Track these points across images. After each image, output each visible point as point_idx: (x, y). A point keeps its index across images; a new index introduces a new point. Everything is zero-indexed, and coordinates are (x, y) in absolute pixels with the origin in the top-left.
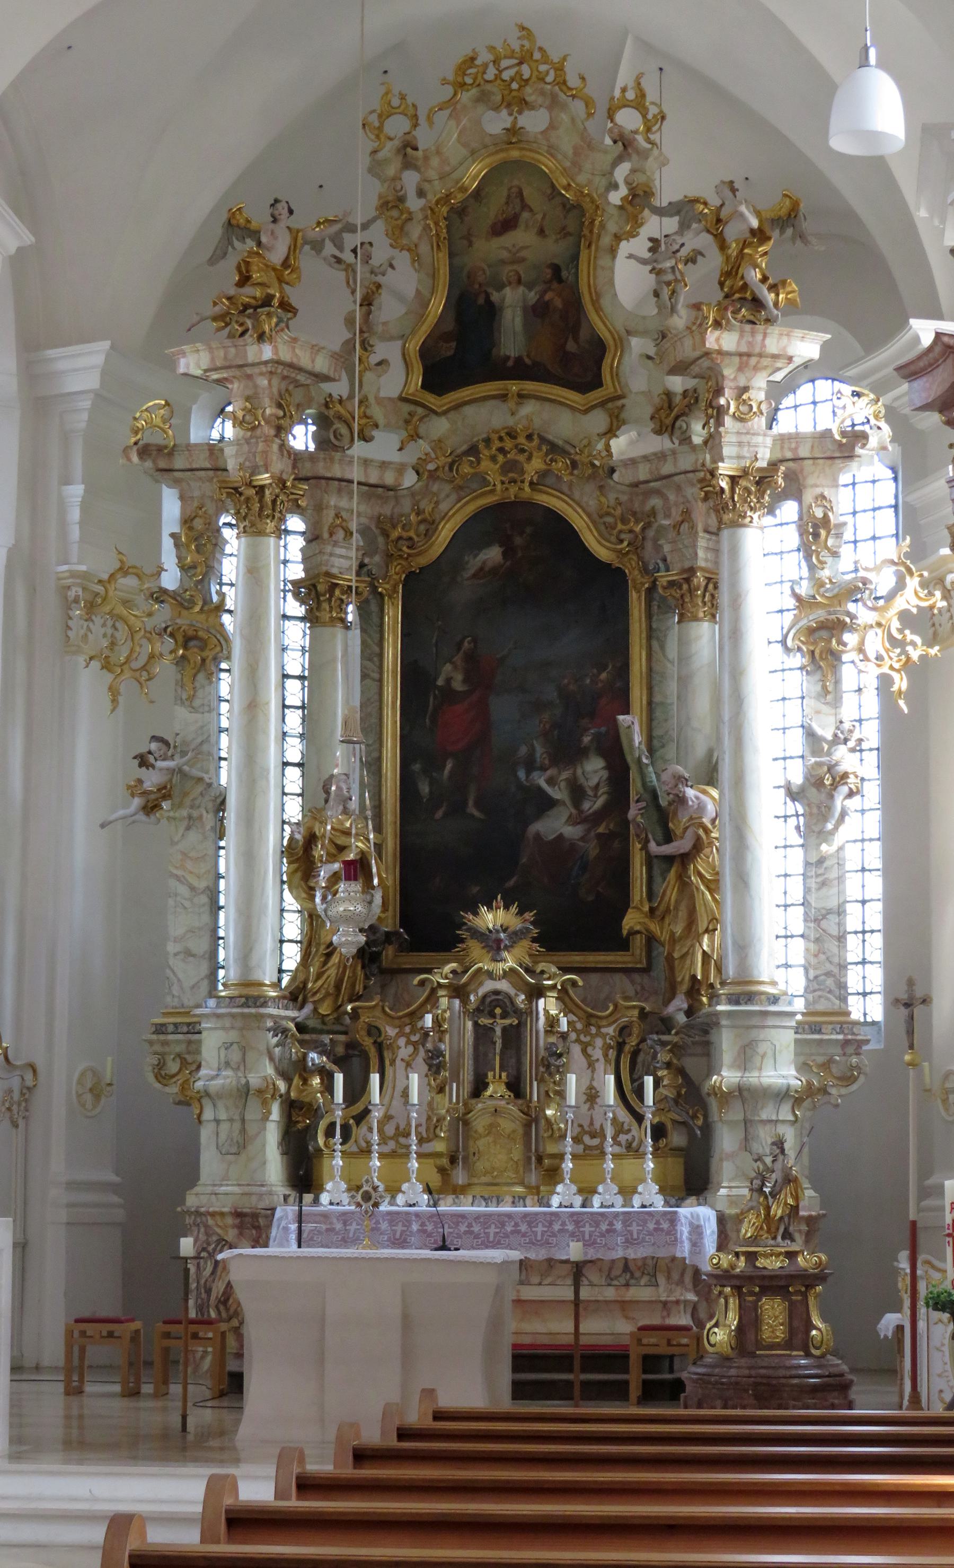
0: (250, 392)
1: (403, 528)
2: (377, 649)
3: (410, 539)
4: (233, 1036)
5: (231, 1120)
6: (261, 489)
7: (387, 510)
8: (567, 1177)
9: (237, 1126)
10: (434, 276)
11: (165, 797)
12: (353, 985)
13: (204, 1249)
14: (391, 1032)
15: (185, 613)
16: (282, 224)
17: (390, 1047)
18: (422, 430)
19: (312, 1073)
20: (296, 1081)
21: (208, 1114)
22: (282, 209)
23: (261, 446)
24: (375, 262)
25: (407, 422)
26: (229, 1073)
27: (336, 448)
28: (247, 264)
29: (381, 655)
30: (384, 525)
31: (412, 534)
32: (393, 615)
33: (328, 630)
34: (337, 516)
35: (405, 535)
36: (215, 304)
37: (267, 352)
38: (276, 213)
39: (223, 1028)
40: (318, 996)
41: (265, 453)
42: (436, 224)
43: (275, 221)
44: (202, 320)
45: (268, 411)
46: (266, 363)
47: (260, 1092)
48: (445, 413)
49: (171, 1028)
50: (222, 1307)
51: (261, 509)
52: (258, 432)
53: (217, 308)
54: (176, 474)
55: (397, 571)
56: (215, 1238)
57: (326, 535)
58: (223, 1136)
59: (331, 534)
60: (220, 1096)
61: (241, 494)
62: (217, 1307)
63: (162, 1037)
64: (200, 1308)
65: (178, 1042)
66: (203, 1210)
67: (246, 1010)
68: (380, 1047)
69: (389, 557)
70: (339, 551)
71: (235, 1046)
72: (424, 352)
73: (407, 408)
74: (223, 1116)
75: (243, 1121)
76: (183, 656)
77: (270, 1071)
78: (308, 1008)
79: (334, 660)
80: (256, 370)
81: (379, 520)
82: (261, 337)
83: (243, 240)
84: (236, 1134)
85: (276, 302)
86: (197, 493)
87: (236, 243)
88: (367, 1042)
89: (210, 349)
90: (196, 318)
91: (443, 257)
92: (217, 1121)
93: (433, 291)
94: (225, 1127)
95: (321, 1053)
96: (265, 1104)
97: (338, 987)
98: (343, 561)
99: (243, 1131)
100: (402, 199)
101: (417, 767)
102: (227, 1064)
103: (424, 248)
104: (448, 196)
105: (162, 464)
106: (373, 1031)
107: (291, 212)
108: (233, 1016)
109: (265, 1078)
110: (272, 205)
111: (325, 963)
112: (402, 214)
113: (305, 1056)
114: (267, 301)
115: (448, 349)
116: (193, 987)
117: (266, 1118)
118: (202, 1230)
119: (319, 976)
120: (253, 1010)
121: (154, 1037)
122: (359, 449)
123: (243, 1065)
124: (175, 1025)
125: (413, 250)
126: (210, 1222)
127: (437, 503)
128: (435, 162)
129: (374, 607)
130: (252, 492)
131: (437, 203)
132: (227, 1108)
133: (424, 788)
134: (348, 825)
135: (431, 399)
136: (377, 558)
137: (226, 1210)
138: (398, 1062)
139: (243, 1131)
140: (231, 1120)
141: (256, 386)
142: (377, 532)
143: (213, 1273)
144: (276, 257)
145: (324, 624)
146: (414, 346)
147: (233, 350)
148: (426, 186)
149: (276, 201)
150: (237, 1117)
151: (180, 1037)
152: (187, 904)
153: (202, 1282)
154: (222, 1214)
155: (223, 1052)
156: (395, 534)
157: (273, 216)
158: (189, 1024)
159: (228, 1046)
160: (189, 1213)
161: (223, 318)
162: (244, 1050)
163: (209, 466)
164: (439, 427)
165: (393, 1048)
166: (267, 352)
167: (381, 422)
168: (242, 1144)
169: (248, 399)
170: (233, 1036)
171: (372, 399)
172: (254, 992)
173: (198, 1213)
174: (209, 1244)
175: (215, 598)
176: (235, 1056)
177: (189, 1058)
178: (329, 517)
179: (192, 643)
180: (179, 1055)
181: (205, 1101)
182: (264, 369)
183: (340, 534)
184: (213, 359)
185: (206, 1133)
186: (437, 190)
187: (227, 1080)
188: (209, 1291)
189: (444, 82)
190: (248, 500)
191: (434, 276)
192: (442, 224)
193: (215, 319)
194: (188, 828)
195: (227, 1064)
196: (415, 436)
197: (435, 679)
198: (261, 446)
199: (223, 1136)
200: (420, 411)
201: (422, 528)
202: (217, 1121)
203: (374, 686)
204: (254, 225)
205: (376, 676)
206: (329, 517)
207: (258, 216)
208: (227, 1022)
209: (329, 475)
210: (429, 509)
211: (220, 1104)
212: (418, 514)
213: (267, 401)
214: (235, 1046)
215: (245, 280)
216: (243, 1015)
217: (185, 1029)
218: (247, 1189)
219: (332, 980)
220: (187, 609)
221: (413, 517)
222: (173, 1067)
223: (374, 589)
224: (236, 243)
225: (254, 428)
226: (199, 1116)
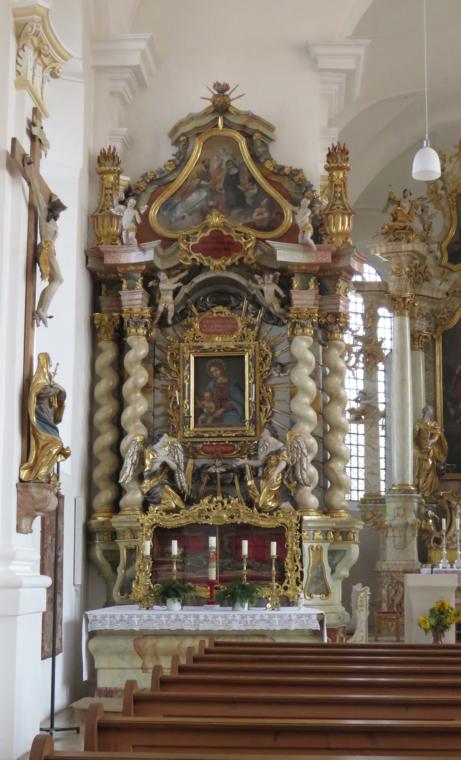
0: (399, 262)
1: (442, 314)
2: (433, 360)
3: (444, 318)
4: (400, 504)
5: (400, 536)
6: (404, 299)
7: (435, 307)
8: (444, 556)
9: (403, 538)
10: (451, 220)
11: (363, 415)
12: (435, 486)
13: (391, 585)
14: (455, 503)
15: (368, 345)
16: (407, 199)
17: (454, 508)
18: (448, 278)
19: (429, 518)
20: (424, 521)
21: (390, 534)
22: (407, 193)
23: (404, 282)
24: (429, 214)
25: (442, 274)
26: (399, 518)
27: (418, 283)
28: (396, 213)
29: (435, 362)
30: (434, 313)
31: (445, 316)
32: (439, 347)
33: (417, 352)
34: (420, 309)
35: (442, 317)
36: (383, 228)
37: (410, 247)
38: (405, 194)
39: (396, 502)
40: (424, 489)
41: (406, 285)
42: (452, 200)
43: (405, 197)
44: (378, 234)
45: (407, 269)
46: (408, 251)
47: (412, 525)
48: (457, 271)
49: (368, 501)
50: (399, 607)
51: (404, 306)
52: (402, 277)
53: (384, 230)
54: (364, 293)
55: (440, 330)
56: (395, 581)
57: (416, 317)
58: (397, 543)
59: (418, 316)
60: (396, 527)
61: (396, 300)
62: (397, 607)
63: (365, 505)
64: (389, 607)
65: (371, 506)
66: (391, 570)
67: (406, 495)
68: (450, 508)
69: (437, 326)
70: (421, 322)
71: (401, 508)
72: (449, 248)
73: (442, 269)
74: (397, 534)
75: (405, 536)
76: (368, 362)
77: (415, 518)
78: (421, 493)
79: (420, 364)
80: (403, 254)
81: (432, 311)
82: (408, 241)
83: (392, 205)
84: (402, 542)
85: (407, 228)
86: (370, 300)
87: (390, 206)
88: (446, 507)
89: (387, 246)
90: (375, 234)
91: (454, 213)
92: (394, 537)
93: (451, 226)
94: (397, 539)
95: (432, 511)
96: (414, 530)
97: (431, 487)
98: (423, 325)
99: (405, 540)
100: (437, 190)
101: (449, 404)
102: (398, 515)
103: (447, 209)
104: (456, 191)
105: (361, 289)
106: (449, 503)
107: (411, 194)
108: (401, 497)
109: (414, 520)
110: (404, 192)
111: (427, 477)
112: (438, 196)
113: (427, 512)
114: (404, 228)
115: (457, 248)
116: (375, 486)
117: (414, 535)
118: (390, 578)
119: (425, 481)
120: (409, 495)
121: (362, 505)
122: (426, 284)
123: (404, 515)
124: (370, 500)
125: (442, 210)
126: (393, 575)
127: (454, 305)
128: (450, 177)
129: (431, 344)
130: (401, 300)
131: (452, 192)
132: (399, 532)
133: (452, 412)
134: (433, 425)
135: (451, 266)
136: (432, 326)
137: (401, 570)
138: (457, 514)
139: (405, 540)
140: (400, 536)
141: (401, 260)
142: (431, 315)
143: (395, 594)
144: (406, 211)
145: (415, 350)
146: (444, 245)
147: (396, 246)
148: (447, 186)
149: (406, 190)
150: (403, 535)
151: (372, 505)
152: (372, 454)
153: (390, 597)
154: (399, 572)
155: (396, 511)
156: (438, 316)
157: (404, 195)
158: (375, 500)
159: (398, 508)
160: (384, 571)
161: (386, 234)
162: (405, 510)
163: (378, 289)
164: (454, 277)
165: (455, 509)
166: (410, 247)
167: (433, 275)
168: (405, 546)
169: (398, 264)
170: (400, 504)
171: (429, 265)
172: (406, 488)
173: (388, 571)
174: (392, 583)
175: (379, 340)
176: (401, 512)
177: (375, 513)
178: (416, 310)
179: (370, 356)
180: (371, 512)
181: (389, 529)
182: (406, 253)
183: (421, 316)
184: (387, 250)
185: (389, 541)
186: (451, 188)
187: (398, 521)
188: (393, 601)
189: (455, 147)
190: (398, 302)
191: (451, 220)
192: (454, 200)
193: (383, 234)
194: (371, 426)
195: (398, 515)
196: (446, 280)
197: (455, 371)
198: (404, 282)
199: (397, 543)
200: (447, 270)
201: (448, 314)
202: (394, 537)
203: (432, 373)
204: (398, 198)
205: (433, 369)
206: (416, 310)
207: (398, 196)
208: (398, 499)
209: (420, 294)
210: (451, 307)
211: (396, 531)
212: (447, 309)
213: (405, 265)
214: (401, 508)
215: (395, 220)
216: (405, 497)
217: (374, 502)
218: (408, 562)
219: (429, 483)
220: (369, 343)
221: (445, 310)
222: (369, 516)
223: (432, 338)
224: (390, 206)
225: (400, 276)
226: (386, 534)
